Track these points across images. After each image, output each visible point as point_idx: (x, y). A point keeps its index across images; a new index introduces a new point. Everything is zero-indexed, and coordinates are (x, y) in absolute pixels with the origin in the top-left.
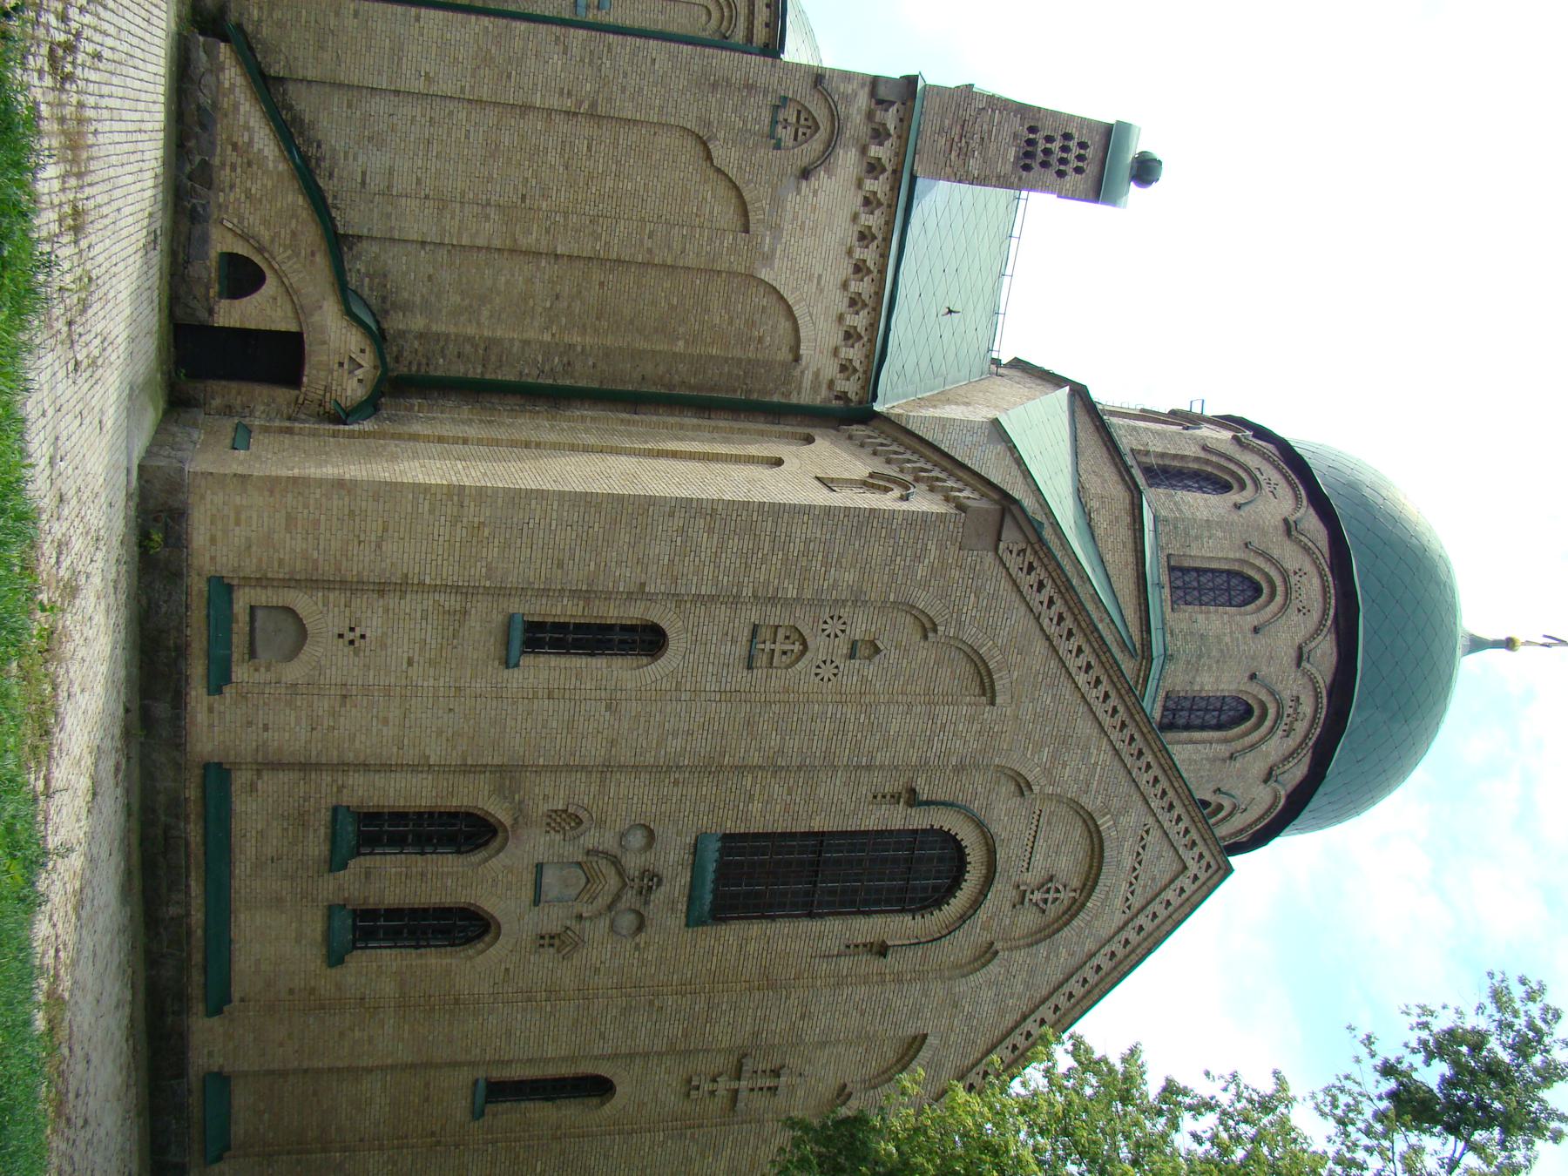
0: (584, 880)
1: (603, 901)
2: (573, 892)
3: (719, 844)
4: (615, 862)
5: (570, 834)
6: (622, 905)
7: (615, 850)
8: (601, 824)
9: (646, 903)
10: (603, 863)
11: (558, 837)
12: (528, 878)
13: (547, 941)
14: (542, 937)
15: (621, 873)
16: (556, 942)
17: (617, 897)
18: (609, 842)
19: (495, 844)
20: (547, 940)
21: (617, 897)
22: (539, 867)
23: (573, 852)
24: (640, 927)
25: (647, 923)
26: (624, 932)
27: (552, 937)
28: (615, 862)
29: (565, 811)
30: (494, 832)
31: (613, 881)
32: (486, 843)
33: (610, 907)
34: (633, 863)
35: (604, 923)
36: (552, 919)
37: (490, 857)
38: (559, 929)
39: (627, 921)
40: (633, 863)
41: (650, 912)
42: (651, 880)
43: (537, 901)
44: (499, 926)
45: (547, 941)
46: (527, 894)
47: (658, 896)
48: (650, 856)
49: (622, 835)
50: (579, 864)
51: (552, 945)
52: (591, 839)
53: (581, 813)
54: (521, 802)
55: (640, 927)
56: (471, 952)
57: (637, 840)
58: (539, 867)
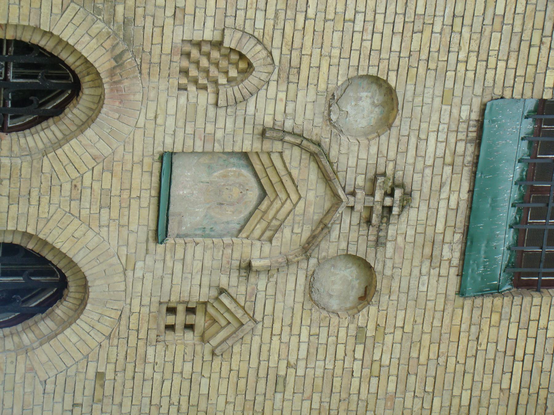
0: (254, 194)
1: (291, 237)
2: (233, 217)
3: (528, 126)
4: (317, 154)
5: (228, 92)
6: (331, 246)
7: (317, 130)
8: (289, 73)
9: (379, 243)
10: (293, 156)
11: (204, 99)
12: (144, 183)
13: (180, 318)
14: (172, 310)
15: (327, 178)
16: (199, 320)
17: (323, 227)
18: (304, 111)
19: (76, 112)
20: (181, 316)
21: (323, 227)
22: (167, 160)
23: (232, 131)
24: (366, 296)
25: (381, 284)
26: (334, 304)
27: (191, 311)
28: (317, 154)
29: (218, 45)
30: (76, 88)
31: (313, 194)
32: (59, 110)
33: (307, 248)
34: (354, 159)
35: (294, 282)
36: (191, 272)
37: (67, 139)
38: (205, 294)
39: (341, 281)
40: (354, 159)
41: (385, 262)
42: (388, 197)
43: (160, 234)
44: (85, 287)
45: (180, 318)
46: (143, 217)
47: (404, 228)
48: (388, 144)
49: (333, 99)
50: (245, 156)
51: (190, 327)
52: (270, 105)
53: (251, 50)
54: (126, 22)
55: (366, 296)
56: (27, 338)
57: (362, 109)
58: (167, 160)
